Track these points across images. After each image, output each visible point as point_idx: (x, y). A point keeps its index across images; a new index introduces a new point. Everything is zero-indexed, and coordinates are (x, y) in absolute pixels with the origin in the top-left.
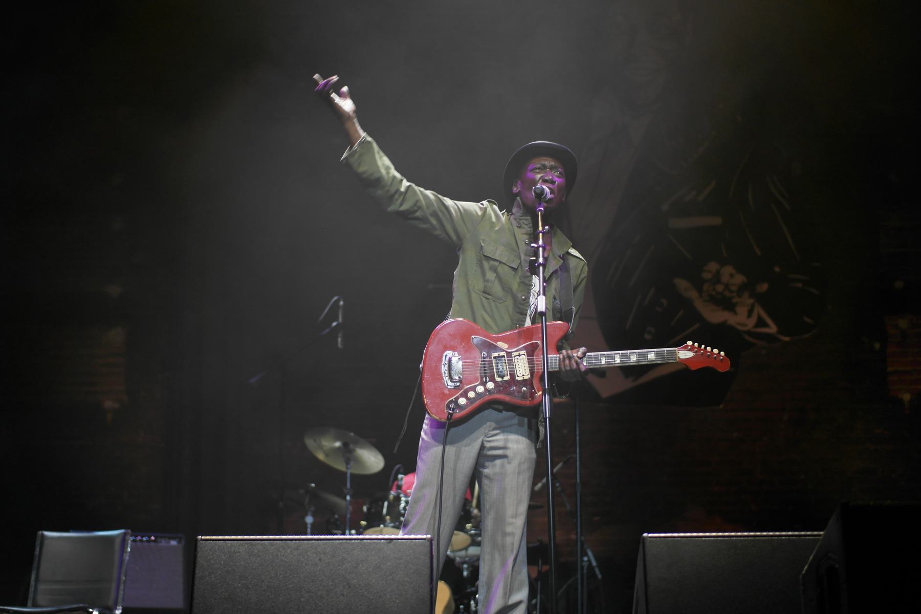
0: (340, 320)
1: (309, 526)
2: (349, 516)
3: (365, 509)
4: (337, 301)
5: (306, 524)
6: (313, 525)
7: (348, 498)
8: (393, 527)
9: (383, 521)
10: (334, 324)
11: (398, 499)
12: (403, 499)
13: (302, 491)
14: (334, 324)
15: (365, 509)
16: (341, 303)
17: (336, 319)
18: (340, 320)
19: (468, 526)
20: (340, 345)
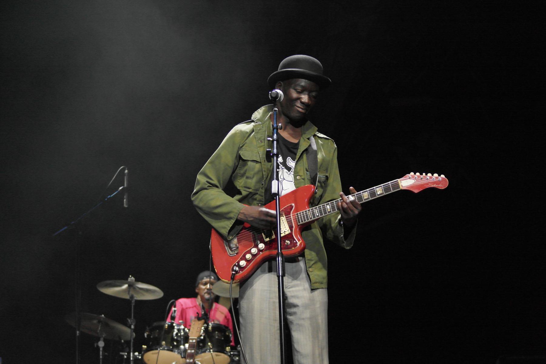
0: (125, 186)
1: (101, 349)
2: (132, 341)
3: (146, 335)
4: (123, 170)
5: (98, 347)
6: (104, 348)
7: (132, 327)
8: (168, 350)
9: (161, 346)
10: (121, 188)
11: (171, 327)
12: (176, 327)
13: (95, 321)
14: (121, 188)
15: (146, 335)
16: (126, 171)
17: (123, 185)
18: (125, 186)
19: (228, 349)
20: (125, 206)
